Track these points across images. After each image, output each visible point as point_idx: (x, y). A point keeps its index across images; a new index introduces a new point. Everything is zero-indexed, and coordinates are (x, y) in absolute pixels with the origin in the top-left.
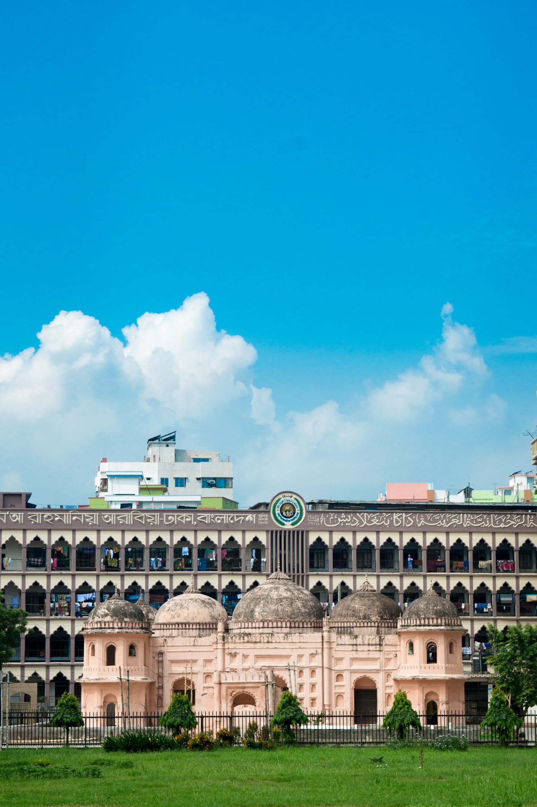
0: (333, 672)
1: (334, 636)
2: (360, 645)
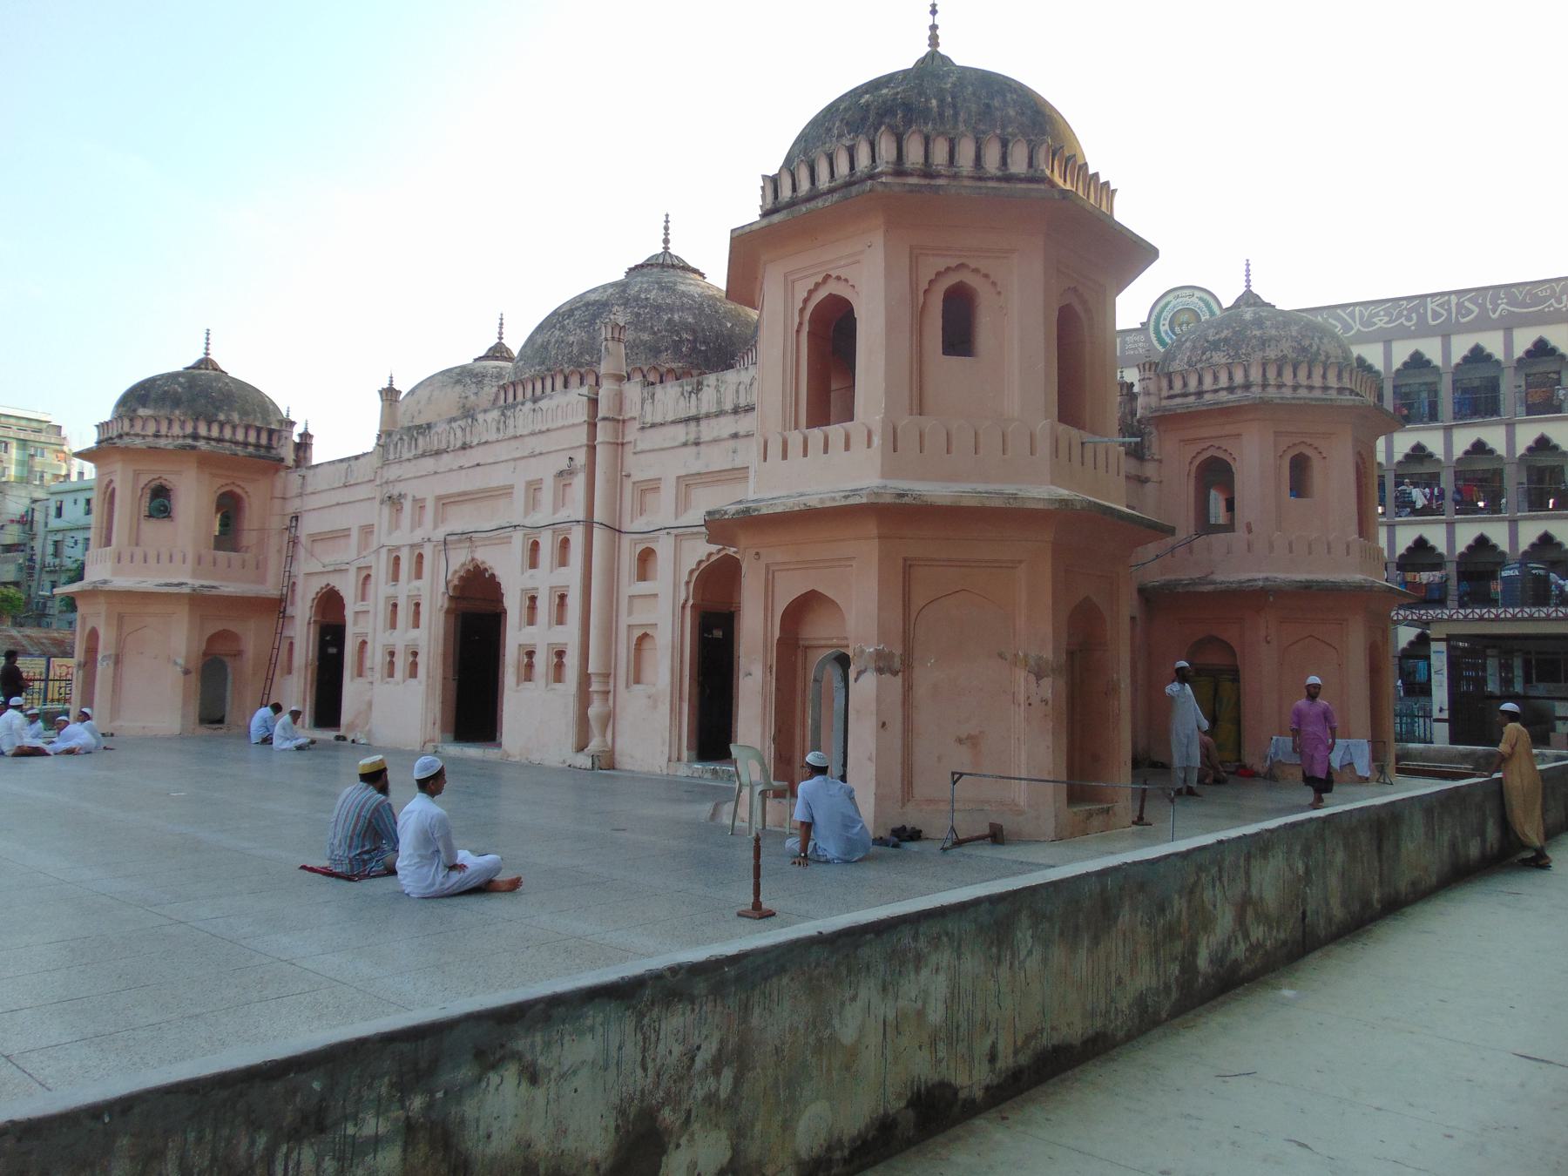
0: (626, 540)
1: (633, 390)
2: (708, 416)
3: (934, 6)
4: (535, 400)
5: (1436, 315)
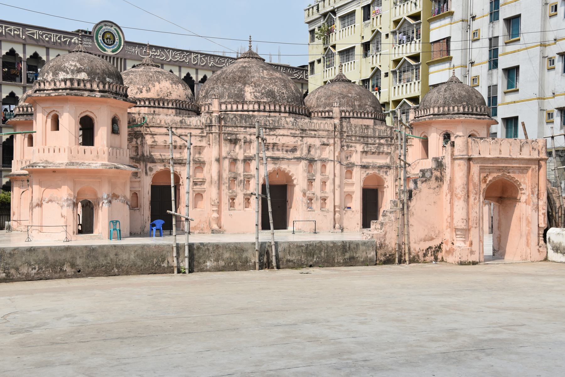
5: (194, 60)
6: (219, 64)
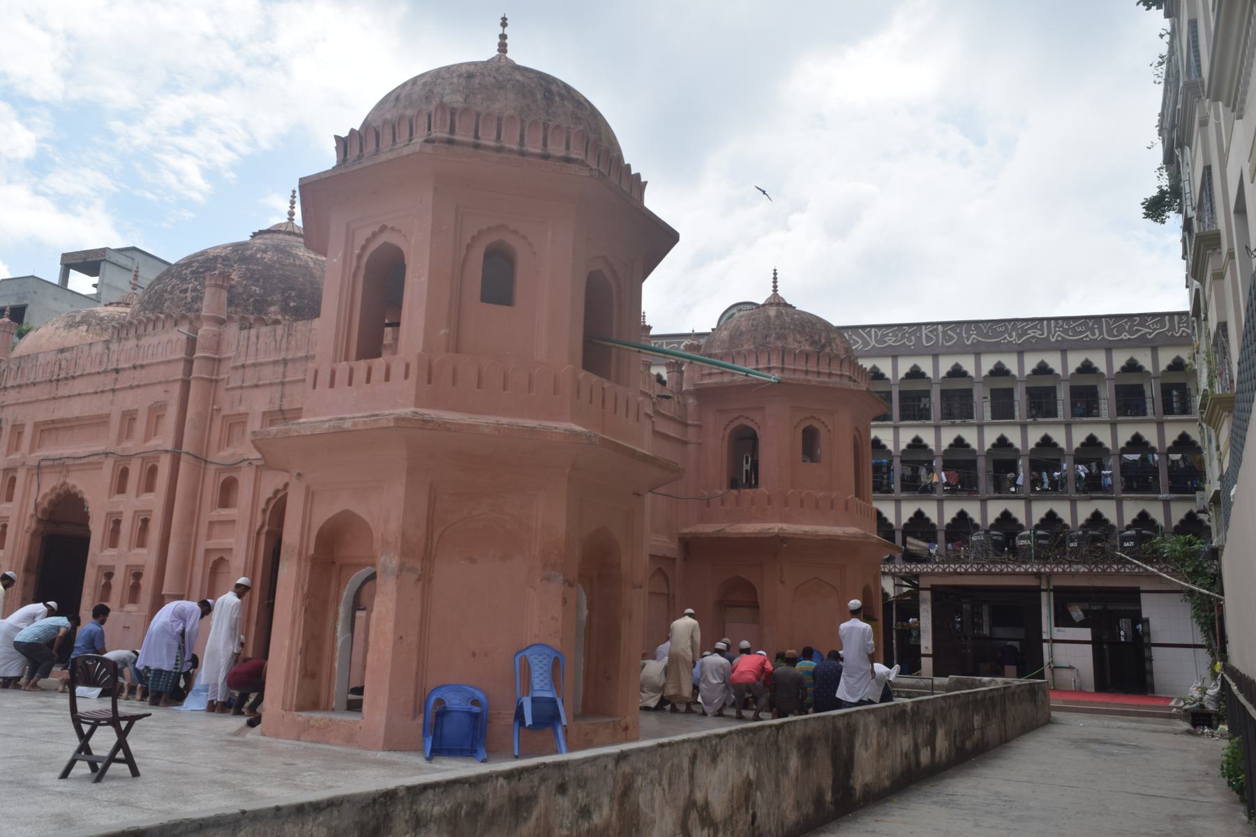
0: (211, 468)
3: (504, 19)
4: (138, 338)
5: (929, 339)
6: (991, 337)
